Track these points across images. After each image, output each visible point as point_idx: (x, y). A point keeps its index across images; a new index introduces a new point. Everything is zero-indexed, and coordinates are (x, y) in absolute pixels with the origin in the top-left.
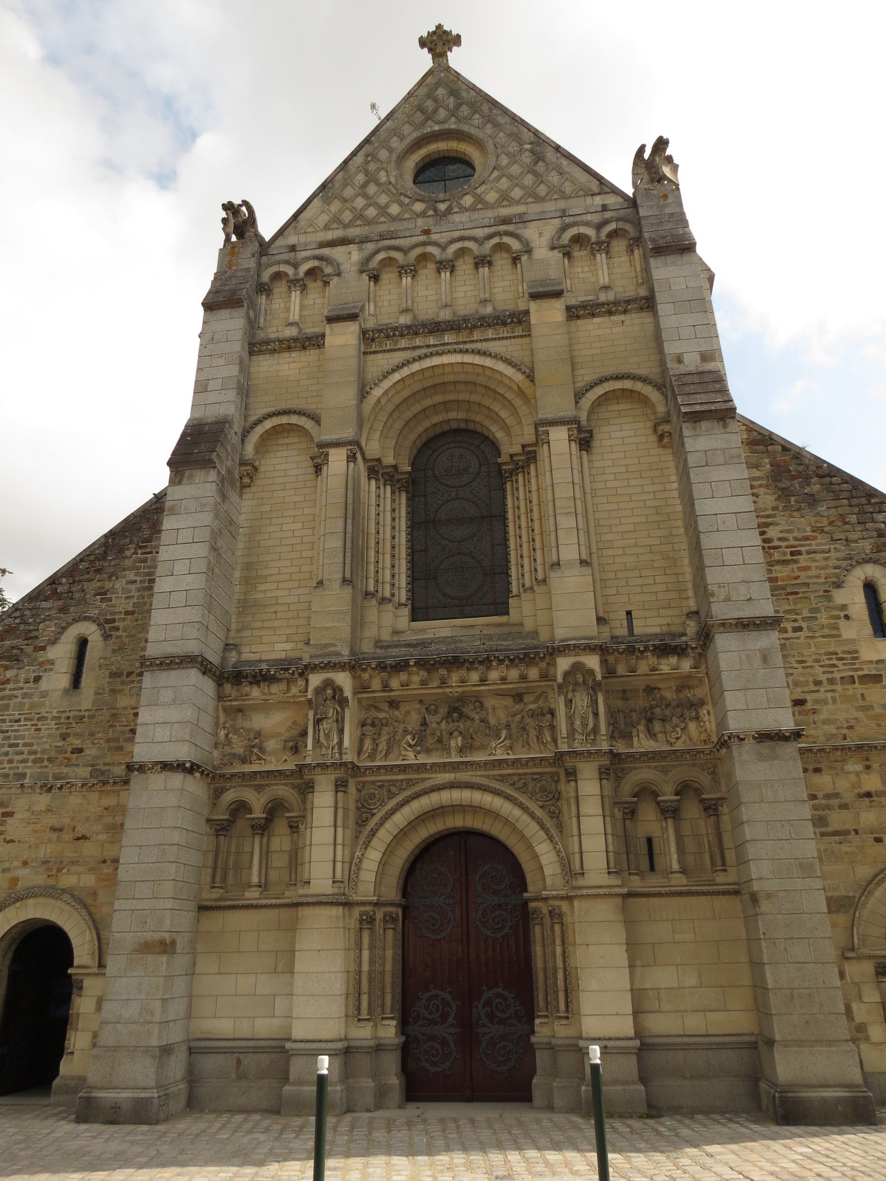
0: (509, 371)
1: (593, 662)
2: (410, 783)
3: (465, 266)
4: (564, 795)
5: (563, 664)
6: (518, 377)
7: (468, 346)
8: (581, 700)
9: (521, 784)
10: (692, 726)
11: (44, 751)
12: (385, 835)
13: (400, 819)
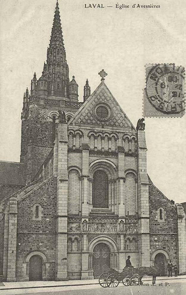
0: (113, 165)
1: (124, 220)
2: (96, 236)
3: (106, 138)
4: (118, 239)
5: (120, 220)
6: (115, 167)
7: (108, 159)
8: (122, 225)
9: (112, 237)
10: (135, 230)
11: (33, 227)
12: (93, 244)
13: (95, 241)
